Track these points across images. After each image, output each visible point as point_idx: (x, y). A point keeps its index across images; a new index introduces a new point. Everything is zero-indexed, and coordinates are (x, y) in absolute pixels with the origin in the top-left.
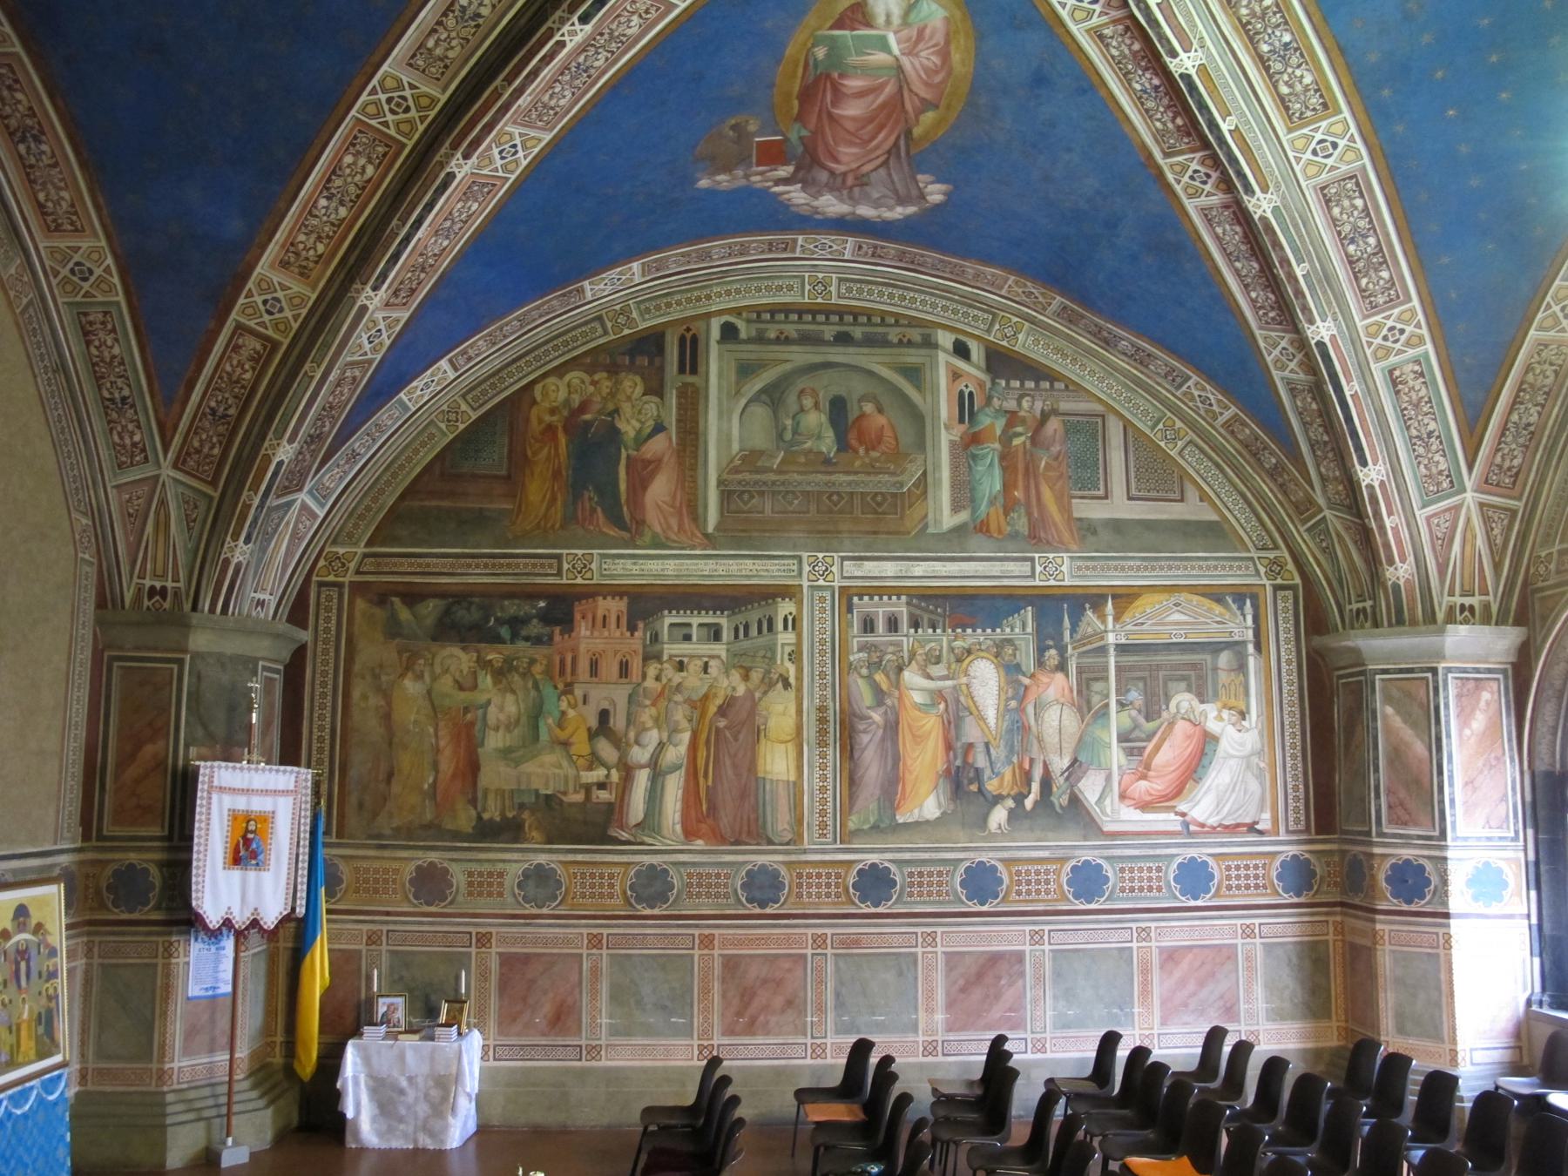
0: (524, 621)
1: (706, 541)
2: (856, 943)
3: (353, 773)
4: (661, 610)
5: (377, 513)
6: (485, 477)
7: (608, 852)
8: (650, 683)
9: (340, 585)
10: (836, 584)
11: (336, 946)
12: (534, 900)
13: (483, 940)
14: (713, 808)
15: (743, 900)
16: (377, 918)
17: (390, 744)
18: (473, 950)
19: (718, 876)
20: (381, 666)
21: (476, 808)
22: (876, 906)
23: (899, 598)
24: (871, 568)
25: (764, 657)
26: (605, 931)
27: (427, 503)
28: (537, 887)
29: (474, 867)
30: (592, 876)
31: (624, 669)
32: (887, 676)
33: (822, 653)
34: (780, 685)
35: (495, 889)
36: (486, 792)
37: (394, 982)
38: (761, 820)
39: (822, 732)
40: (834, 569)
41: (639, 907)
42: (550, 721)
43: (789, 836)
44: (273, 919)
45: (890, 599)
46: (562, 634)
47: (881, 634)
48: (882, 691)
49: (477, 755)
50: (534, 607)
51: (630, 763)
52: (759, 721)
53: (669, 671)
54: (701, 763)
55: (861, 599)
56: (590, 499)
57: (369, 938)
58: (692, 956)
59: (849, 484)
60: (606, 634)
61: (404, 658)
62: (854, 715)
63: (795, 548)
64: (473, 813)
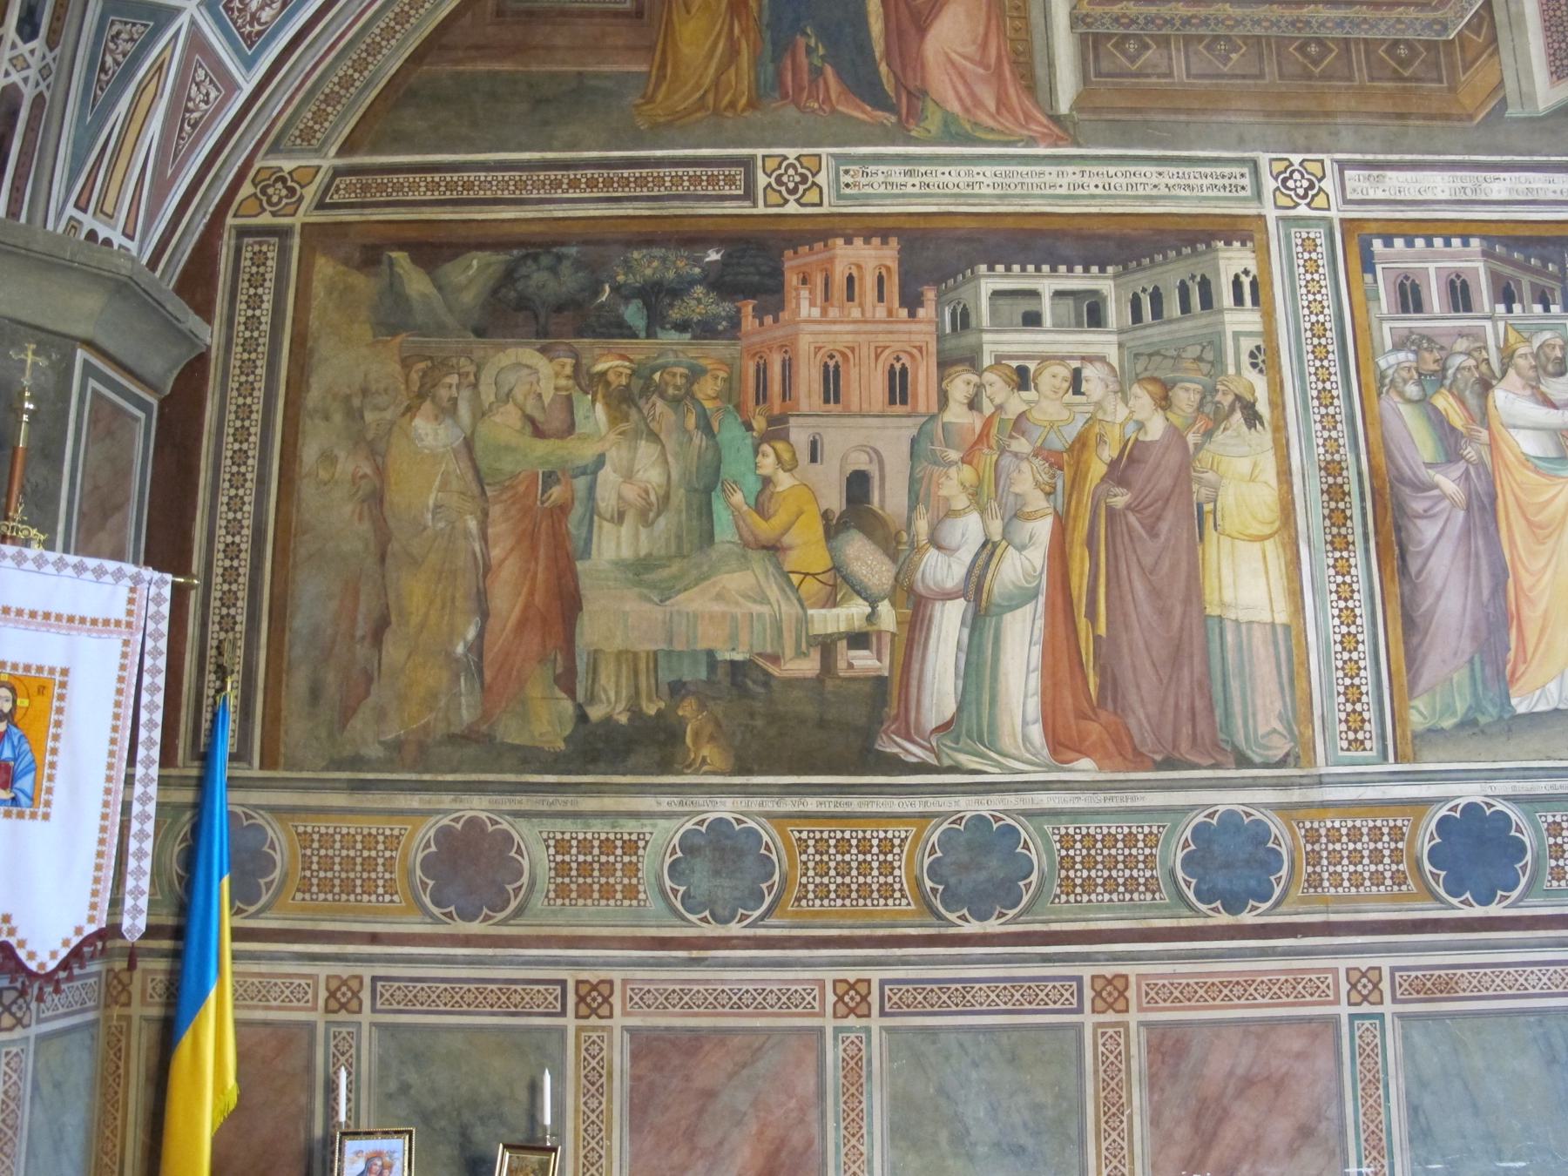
0: (678, 291)
1: (1056, 130)
2: (1445, 988)
3: (299, 623)
4: (972, 265)
5: (361, 92)
6: (589, 14)
7: (880, 790)
8: (957, 414)
9: (283, 233)
10: (1335, 214)
11: (259, 1015)
12: (709, 904)
13: (593, 999)
14: (1111, 685)
15: (1191, 895)
16: (350, 949)
17: (383, 559)
18: (570, 1022)
19: (1130, 839)
20: (365, 392)
21: (571, 693)
22: (1485, 901)
23: (1466, 244)
24: (1399, 184)
25: (1199, 359)
26: (875, 975)
27: (468, 67)
28: (717, 873)
29: (569, 828)
30: (843, 845)
31: (899, 387)
32: (1462, 401)
33: (1320, 353)
34: (1238, 416)
35: (618, 879)
36: (595, 657)
37: (390, 1096)
38: (1219, 712)
39: (1338, 518)
40: (1327, 185)
41: (952, 917)
42: (738, 498)
43: (1281, 747)
44: (56, 944)
45: (1448, 244)
46: (759, 313)
47: (1437, 316)
48: (1453, 429)
49: (575, 576)
50: (697, 261)
51: (920, 588)
52: (1200, 493)
53: (997, 389)
54: (1079, 584)
55: (1388, 242)
56: (809, 51)
57: (332, 994)
58: (1079, 1028)
59: (1340, 24)
60: (856, 313)
61: (415, 377)
62: (1401, 479)
63: (1241, 143)
64: (568, 706)
